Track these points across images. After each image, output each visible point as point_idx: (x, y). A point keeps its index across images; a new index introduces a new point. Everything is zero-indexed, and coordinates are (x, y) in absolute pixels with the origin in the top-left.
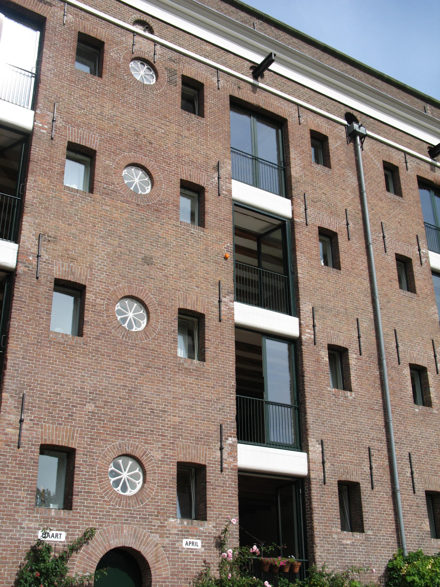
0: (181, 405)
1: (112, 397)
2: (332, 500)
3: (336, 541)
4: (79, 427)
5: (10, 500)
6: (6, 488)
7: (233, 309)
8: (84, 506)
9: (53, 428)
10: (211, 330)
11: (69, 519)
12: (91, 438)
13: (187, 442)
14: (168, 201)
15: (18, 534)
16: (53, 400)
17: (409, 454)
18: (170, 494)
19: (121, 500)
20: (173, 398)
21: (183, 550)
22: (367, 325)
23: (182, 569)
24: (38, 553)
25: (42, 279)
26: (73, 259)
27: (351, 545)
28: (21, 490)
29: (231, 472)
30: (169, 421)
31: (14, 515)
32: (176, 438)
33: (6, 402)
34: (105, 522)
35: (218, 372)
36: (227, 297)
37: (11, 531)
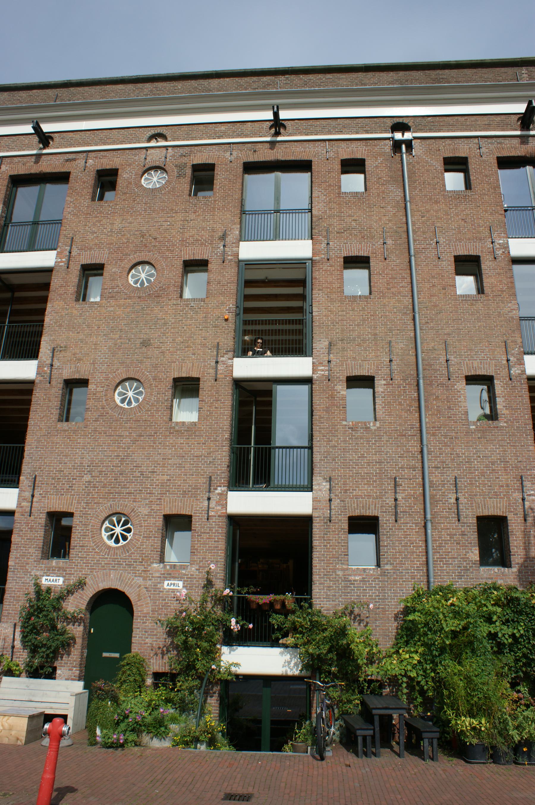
0: (170, 464)
1: (106, 466)
2: (339, 537)
3: (341, 578)
4: (77, 495)
5: (23, 555)
6: (20, 547)
7: (232, 366)
8: (79, 557)
9: (56, 498)
10: (205, 391)
11: (66, 568)
12: (86, 503)
13: (175, 497)
14: (169, 285)
15: (28, 580)
16: (58, 476)
17: (456, 478)
18: (155, 543)
19: (109, 551)
20: (163, 459)
21: (165, 591)
22: (401, 345)
23: (162, 606)
24: (41, 593)
25: (54, 383)
26: (80, 360)
27: (361, 581)
28: (31, 547)
29: (218, 519)
30: (158, 480)
31: (26, 566)
32: (163, 494)
33: (23, 483)
34: (96, 569)
35: (210, 428)
36: (226, 356)
37: (23, 577)
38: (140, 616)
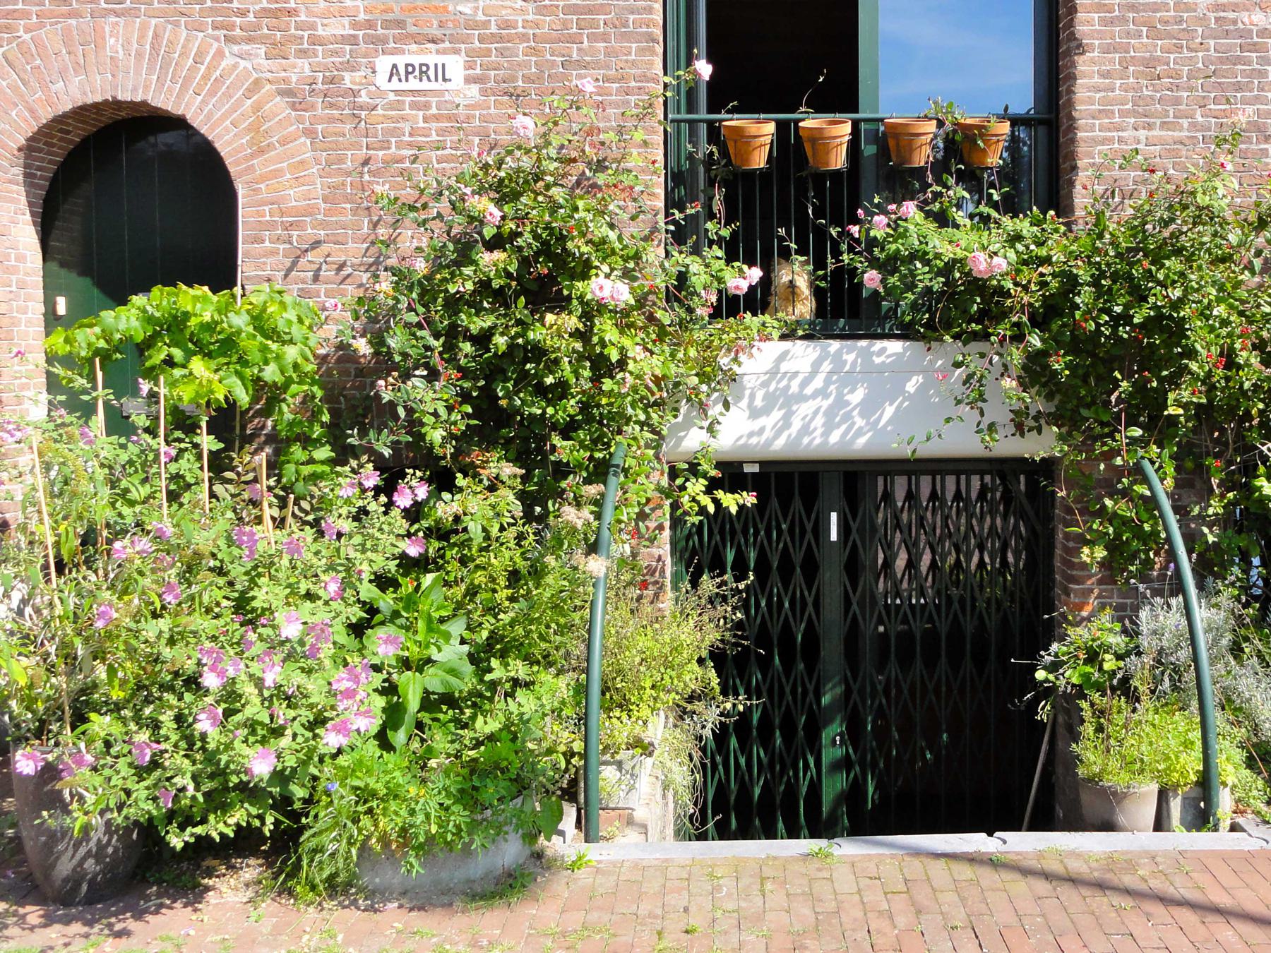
38: (271, 226)
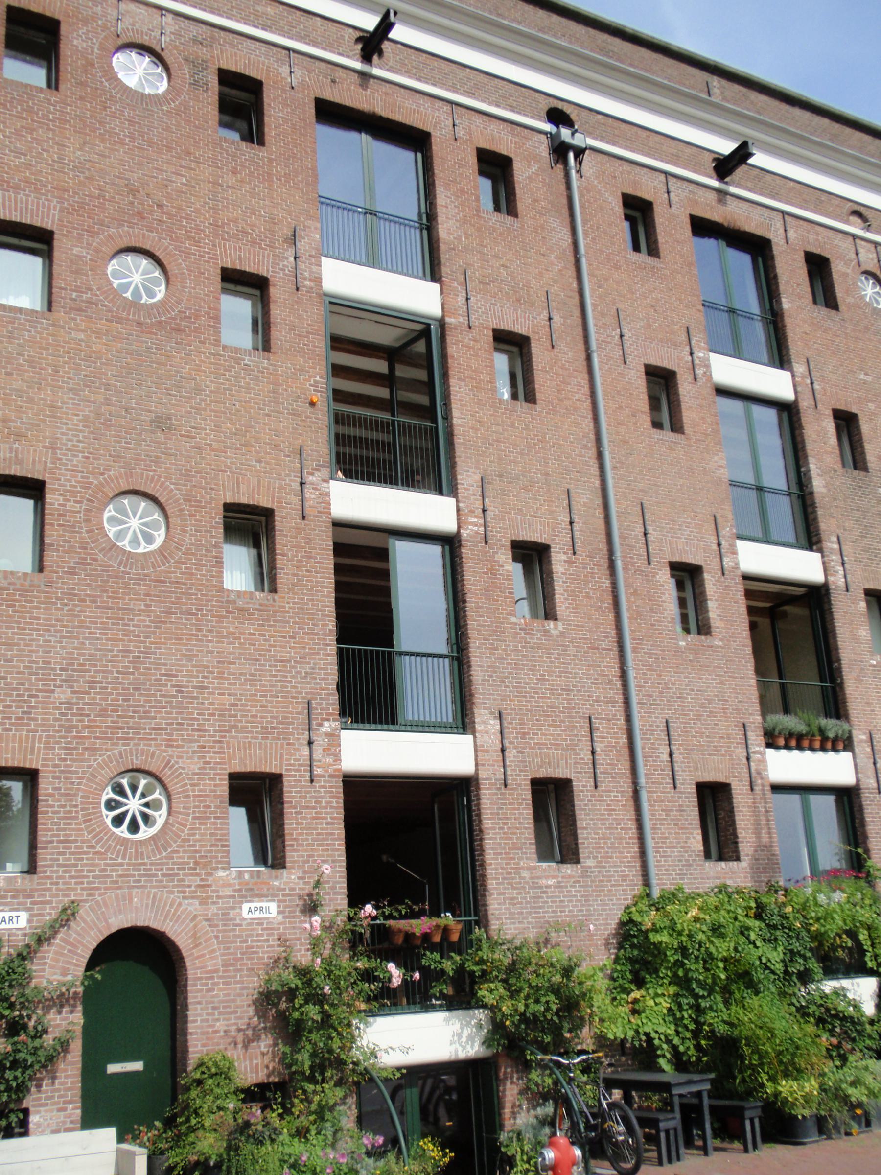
0: (233, 674)
1: (104, 672)
2: (520, 814)
3: (527, 883)
4: (43, 731)
7: (328, 494)
10: (286, 536)
11: (32, 890)
13: (247, 738)
14: (196, 310)
17: (667, 722)
18: (216, 829)
19: (126, 850)
20: (218, 662)
21: (244, 923)
22: (586, 497)
23: (242, 954)
26: (19, 435)
27: (555, 887)
29: (329, 782)
35: (302, 609)
36: (317, 474)
38: (200, 978)
